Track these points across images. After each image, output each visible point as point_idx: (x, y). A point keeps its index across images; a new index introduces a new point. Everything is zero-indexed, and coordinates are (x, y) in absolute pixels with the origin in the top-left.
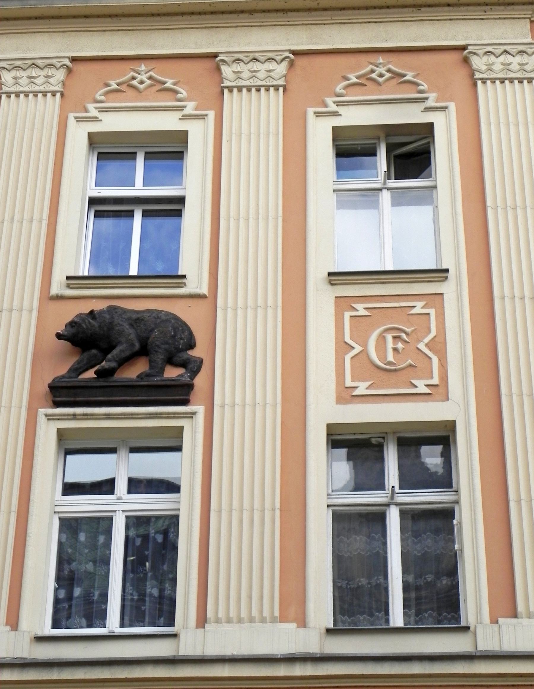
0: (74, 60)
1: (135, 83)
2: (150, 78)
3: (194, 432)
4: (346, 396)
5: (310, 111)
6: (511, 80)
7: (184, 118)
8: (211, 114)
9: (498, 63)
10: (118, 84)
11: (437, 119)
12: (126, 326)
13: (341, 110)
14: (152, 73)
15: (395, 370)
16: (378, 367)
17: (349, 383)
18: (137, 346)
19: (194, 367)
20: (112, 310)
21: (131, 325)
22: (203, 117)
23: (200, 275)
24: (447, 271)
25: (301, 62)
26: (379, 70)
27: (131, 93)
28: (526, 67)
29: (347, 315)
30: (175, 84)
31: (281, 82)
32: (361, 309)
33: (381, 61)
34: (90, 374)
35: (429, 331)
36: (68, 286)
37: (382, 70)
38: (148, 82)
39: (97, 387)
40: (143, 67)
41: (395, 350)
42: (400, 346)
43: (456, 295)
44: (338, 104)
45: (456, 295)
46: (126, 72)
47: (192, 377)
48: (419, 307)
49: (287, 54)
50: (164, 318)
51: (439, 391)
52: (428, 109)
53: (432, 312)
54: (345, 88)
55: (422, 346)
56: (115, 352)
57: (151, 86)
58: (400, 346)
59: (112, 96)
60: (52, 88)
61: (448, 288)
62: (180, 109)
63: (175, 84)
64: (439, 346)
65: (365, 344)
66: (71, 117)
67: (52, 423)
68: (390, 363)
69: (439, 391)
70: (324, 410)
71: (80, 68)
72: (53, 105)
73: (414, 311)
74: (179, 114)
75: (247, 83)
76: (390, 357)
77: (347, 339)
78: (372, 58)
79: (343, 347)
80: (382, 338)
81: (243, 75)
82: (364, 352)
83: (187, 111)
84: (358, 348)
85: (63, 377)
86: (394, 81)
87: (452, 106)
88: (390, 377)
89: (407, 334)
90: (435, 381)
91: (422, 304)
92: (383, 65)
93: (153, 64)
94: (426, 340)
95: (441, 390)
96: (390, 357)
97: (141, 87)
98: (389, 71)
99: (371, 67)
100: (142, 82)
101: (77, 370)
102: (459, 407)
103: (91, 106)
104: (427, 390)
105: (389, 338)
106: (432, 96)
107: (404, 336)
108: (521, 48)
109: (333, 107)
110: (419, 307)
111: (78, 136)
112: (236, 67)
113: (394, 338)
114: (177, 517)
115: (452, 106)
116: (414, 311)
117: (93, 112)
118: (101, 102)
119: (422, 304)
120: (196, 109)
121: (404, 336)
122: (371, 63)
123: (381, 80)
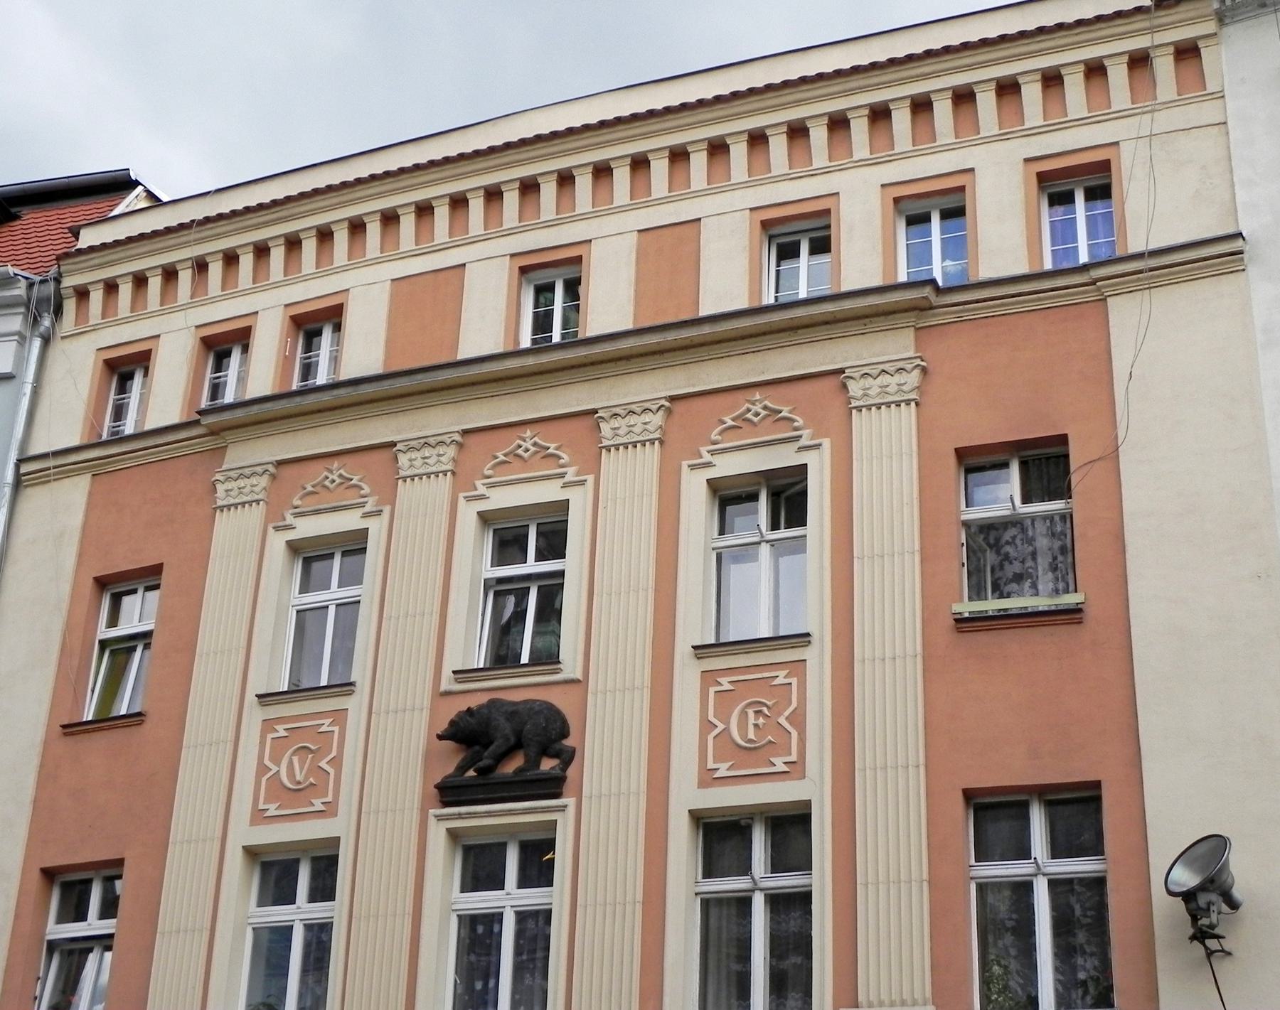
0: (465, 432)
1: (520, 451)
2: (535, 444)
3: (565, 827)
4: (708, 779)
5: (685, 464)
6: (888, 405)
7: (565, 486)
8: (590, 479)
9: (874, 385)
10: (505, 455)
11: (808, 458)
12: (502, 720)
13: (716, 460)
14: (536, 439)
15: (755, 748)
17: (711, 765)
18: (513, 740)
19: (567, 757)
20: (492, 702)
21: (507, 719)
22: (582, 483)
23: (575, 660)
24: (808, 635)
25: (679, 407)
26: (758, 408)
27: (517, 463)
28: (904, 388)
29: (712, 690)
30: (557, 449)
31: (657, 435)
33: (758, 397)
34: (471, 773)
35: (790, 703)
36: (458, 681)
37: (758, 408)
38: (533, 449)
39: (480, 785)
40: (528, 433)
41: (756, 725)
42: (761, 721)
43: (818, 659)
44: (712, 453)
45: (818, 659)
46: (513, 440)
47: (564, 769)
48: (781, 677)
49: (663, 402)
50: (537, 708)
51: (796, 770)
52: (801, 449)
53: (794, 681)
54: (720, 434)
55: (782, 720)
56: (492, 748)
57: (536, 453)
59: (499, 469)
60: (444, 468)
61: (809, 654)
62: (562, 476)
63: (557, 449)
64: (798, 719)
65: (727, 723)
66: (461, 495)
67: (441, 823)
68: (750, 741)
69: (796, 770)
70: (687, 795)
71: (472, 440)
72: (446, 483)
73: (776, 682)
74: (560, 482)
75: (625, 440)
76: (751, 735)
78: (747, 394)
79: (706, 725)
80: (744, 714)
81: (621, 432)
82: (727, 730)
83: (568, 478)
84: (721, 726)
85: (450, 776)
86: (771, 419)
87: (826, 443)
88: (750, 757)
90: (793, 758)
91: (785, 672)
92: (758, 403)
93: (538, 428)
94: (787, 713)
97: (526, 455)
98: (765, 408)
99: (747, 405)
100: (527, 450)
101: (462, 769)
102: (813, 789)
103: (479, 483)
104: (785, 769)
105: (751, 713)
106: (806, 433)
107: (765, 709)
108: (900, 365)
109: (707, 458)
110: (781, 677)
111: (468, 515)
112: (615, 423)
113: (756, 712)
114: (550, 911)
115: (826, 443)
116: (776, 682)
117: (482, 490)
118: (489, 477)
119: (785, 672)
120: (577, 475)
121: (765, 709)
122: (748, 401)
123: (756, 419)
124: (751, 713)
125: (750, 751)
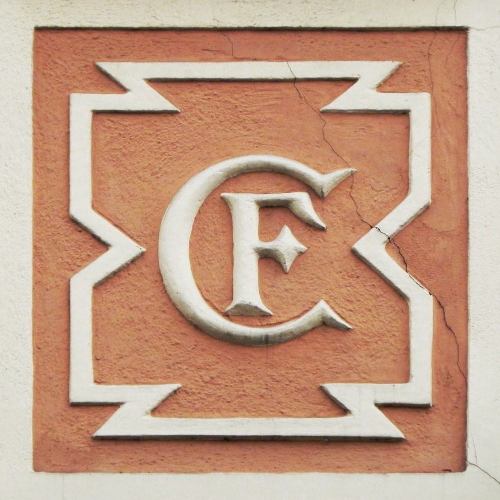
15: (266, 342)
16: (199, 327)
29: (83, 105)
32: (137, 84)
35: (404, 187)
42: (287, 243)
53: (419, 105)
55: (372, 246)
58: (287, 243)
65: (149, 234)
68: (245, 313)
73: (346, 101)
77: (82, 207)
80: (216, 212)
82: (146, 264)
84: (122, 249)
89: (316, 194)
90: (419, 388)
91: (384, 68)
94: (392, 223)
95: (437, 427)
96: (248, 288)
104: (386, 427)
105: (245, 206)
107: (303, 202)
113: (265, 207)
116: (346, 101)
119: (384, 68)
121: (303, 202)
124: (245, 206)
125: (237, 351)
